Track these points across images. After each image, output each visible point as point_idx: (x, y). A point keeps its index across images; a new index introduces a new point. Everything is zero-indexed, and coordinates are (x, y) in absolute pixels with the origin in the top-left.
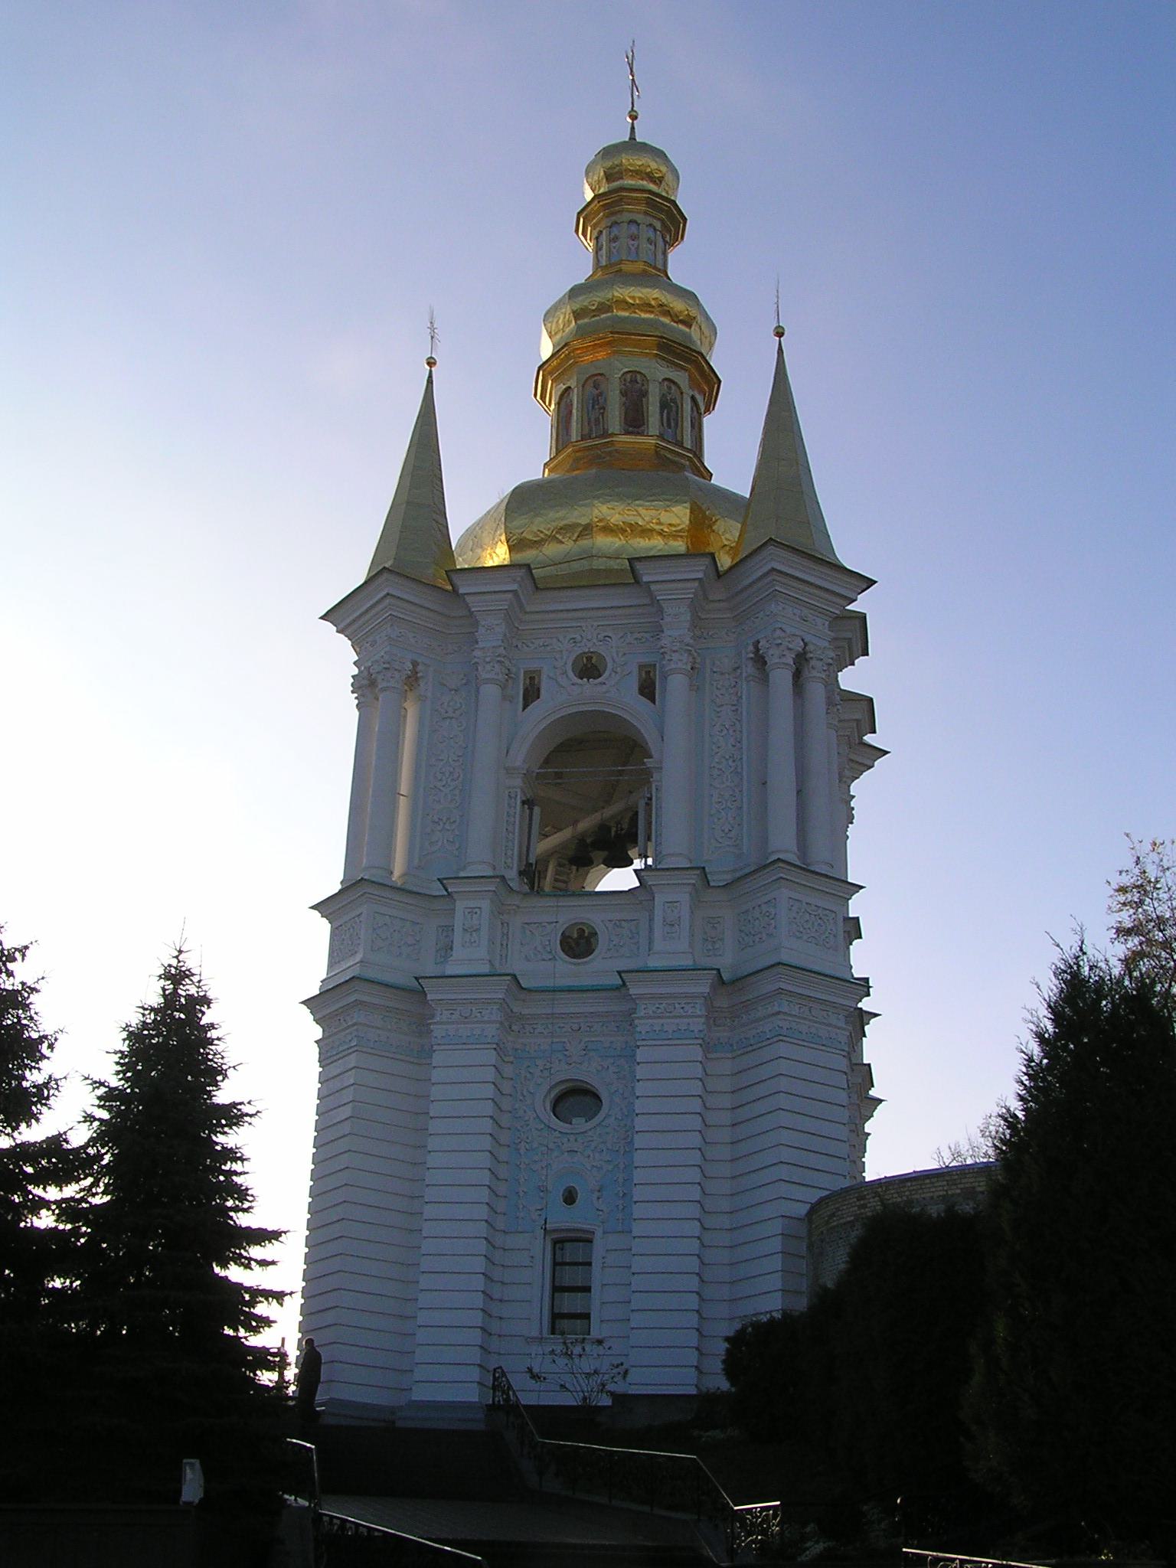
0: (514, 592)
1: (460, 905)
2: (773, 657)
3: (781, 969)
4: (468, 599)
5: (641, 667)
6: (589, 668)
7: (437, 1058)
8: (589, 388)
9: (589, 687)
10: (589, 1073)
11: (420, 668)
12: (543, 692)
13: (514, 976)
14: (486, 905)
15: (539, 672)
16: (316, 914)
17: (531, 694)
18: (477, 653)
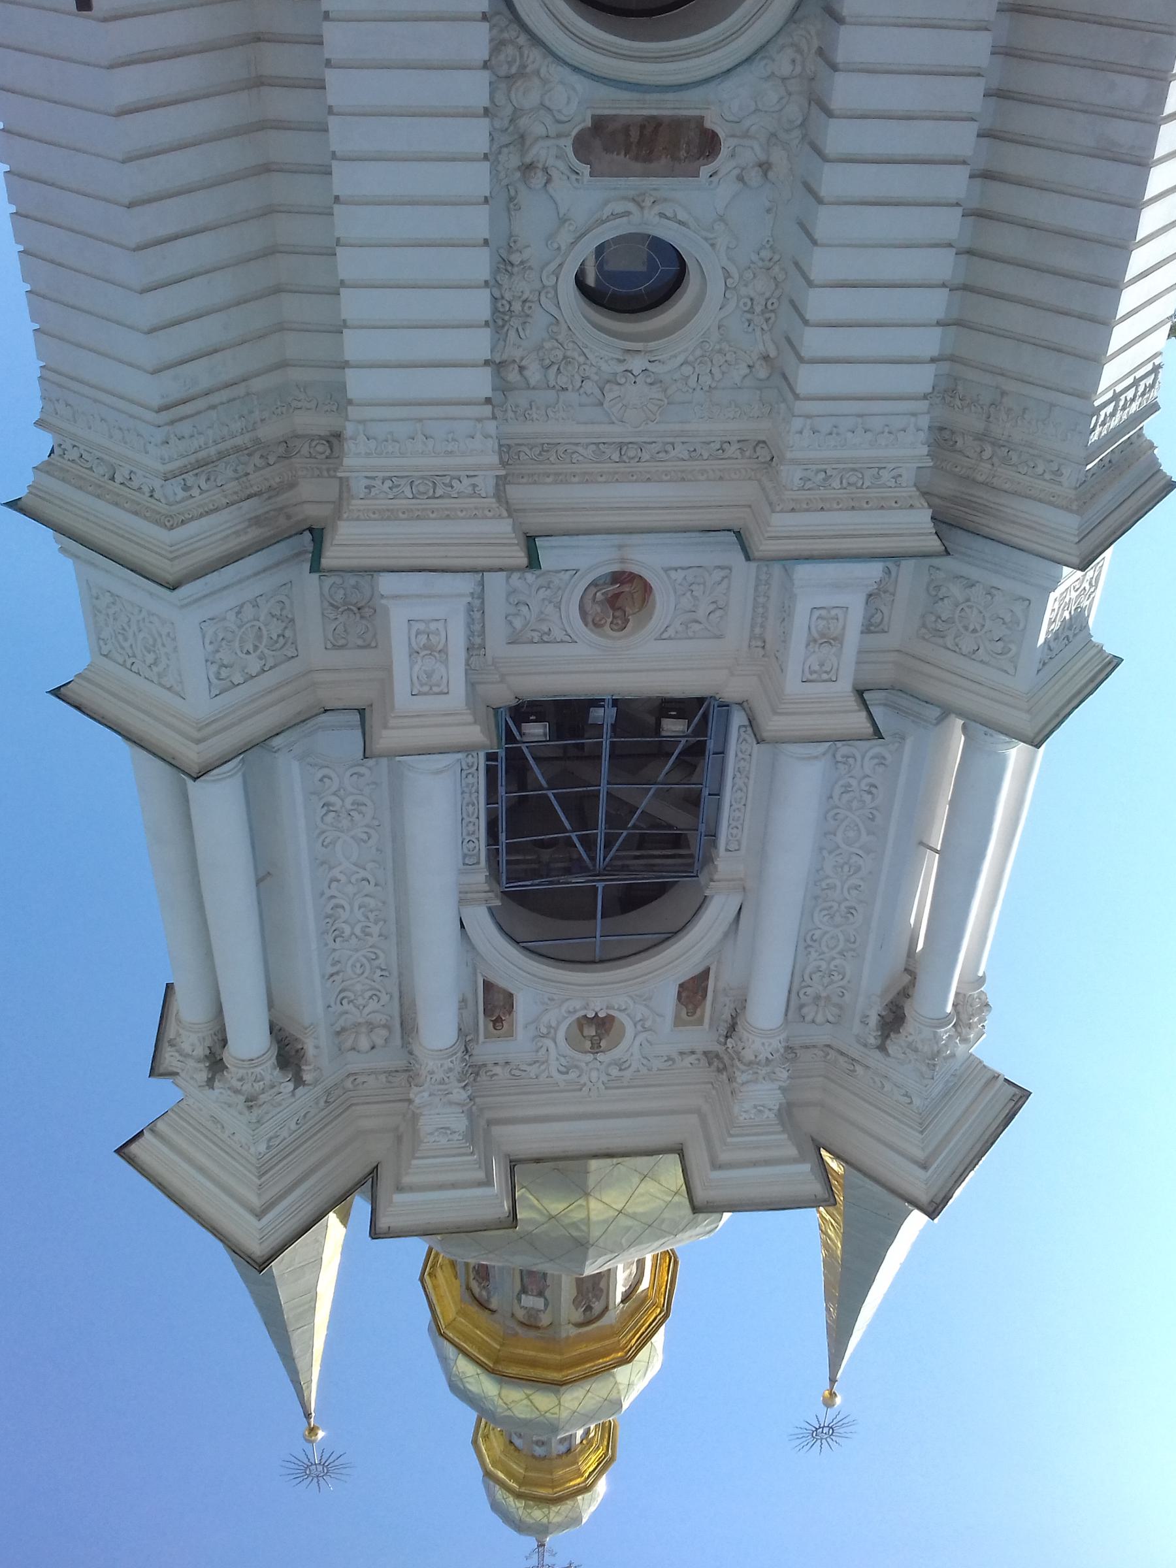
0: (716, 1166)
1: (845, 686)
2: (268, 1070)
3: (170, 575)
4: (793, 1151)
5: (511, 1034)
6: (598, 1029)
7: (923, 378)
8: (597, 1307)
9: (598, 1006)
10: (595, 340)
11: (879, 1042)
12: (673, 991)
13: (748, 558)
14: (792, 685)
15: (678, 1022)
16: (1110, 649)
17: (693, 991)
18: (785, 1075)
